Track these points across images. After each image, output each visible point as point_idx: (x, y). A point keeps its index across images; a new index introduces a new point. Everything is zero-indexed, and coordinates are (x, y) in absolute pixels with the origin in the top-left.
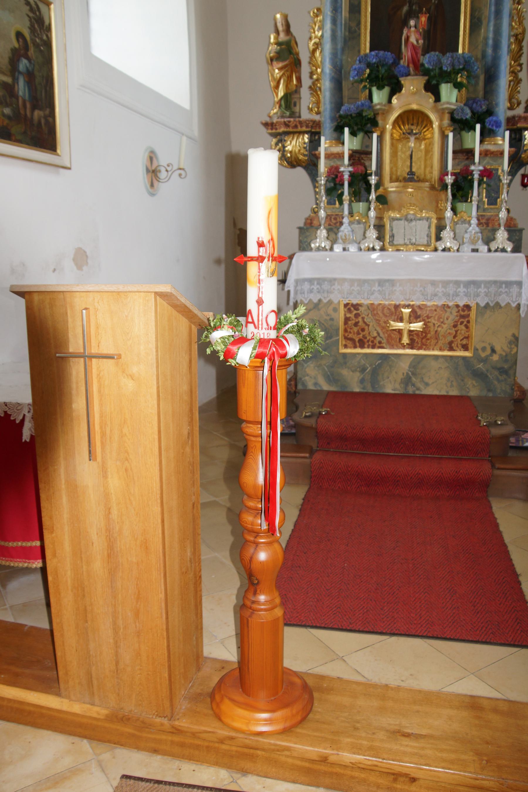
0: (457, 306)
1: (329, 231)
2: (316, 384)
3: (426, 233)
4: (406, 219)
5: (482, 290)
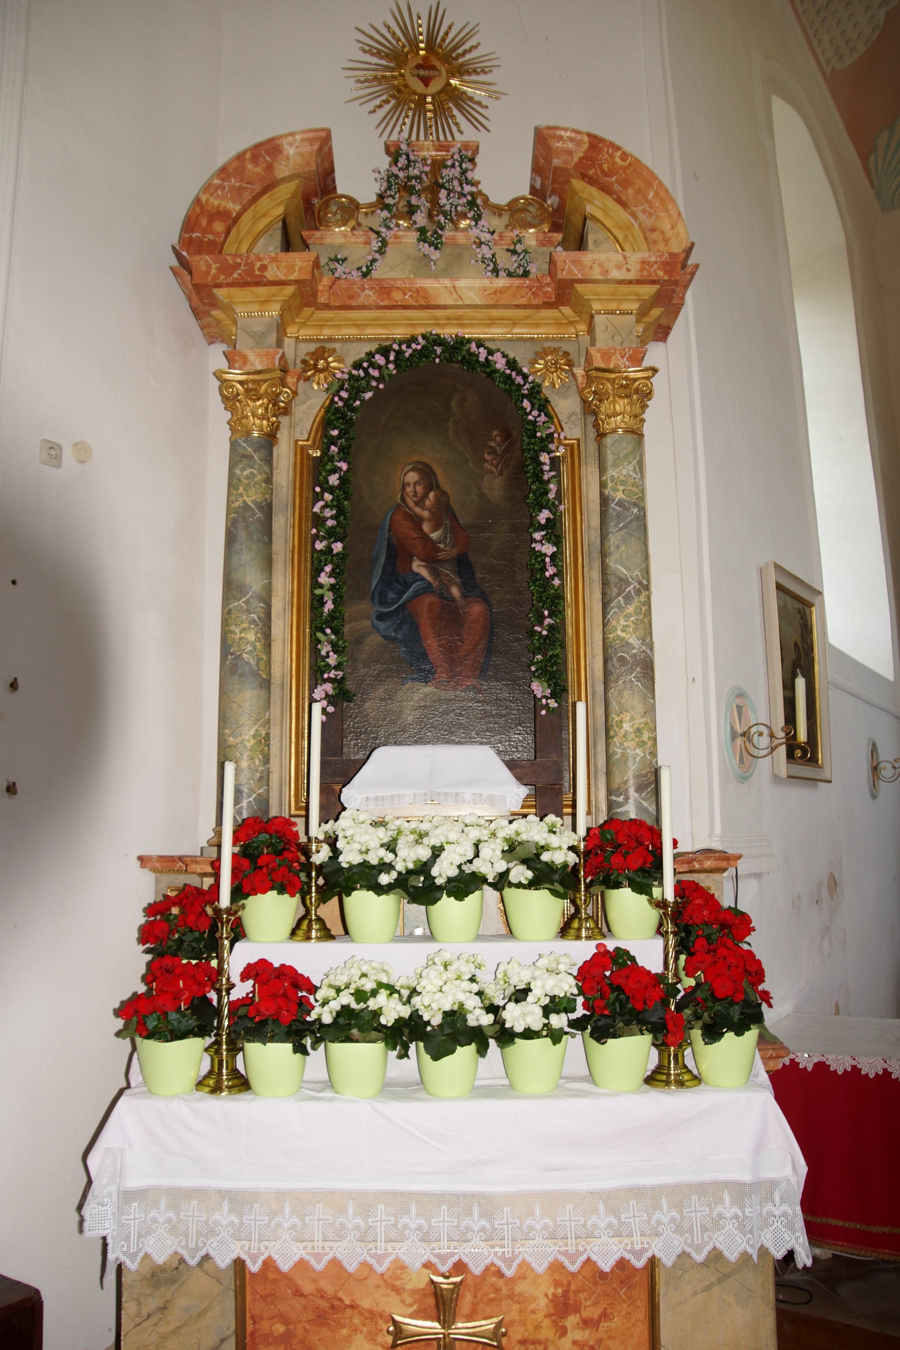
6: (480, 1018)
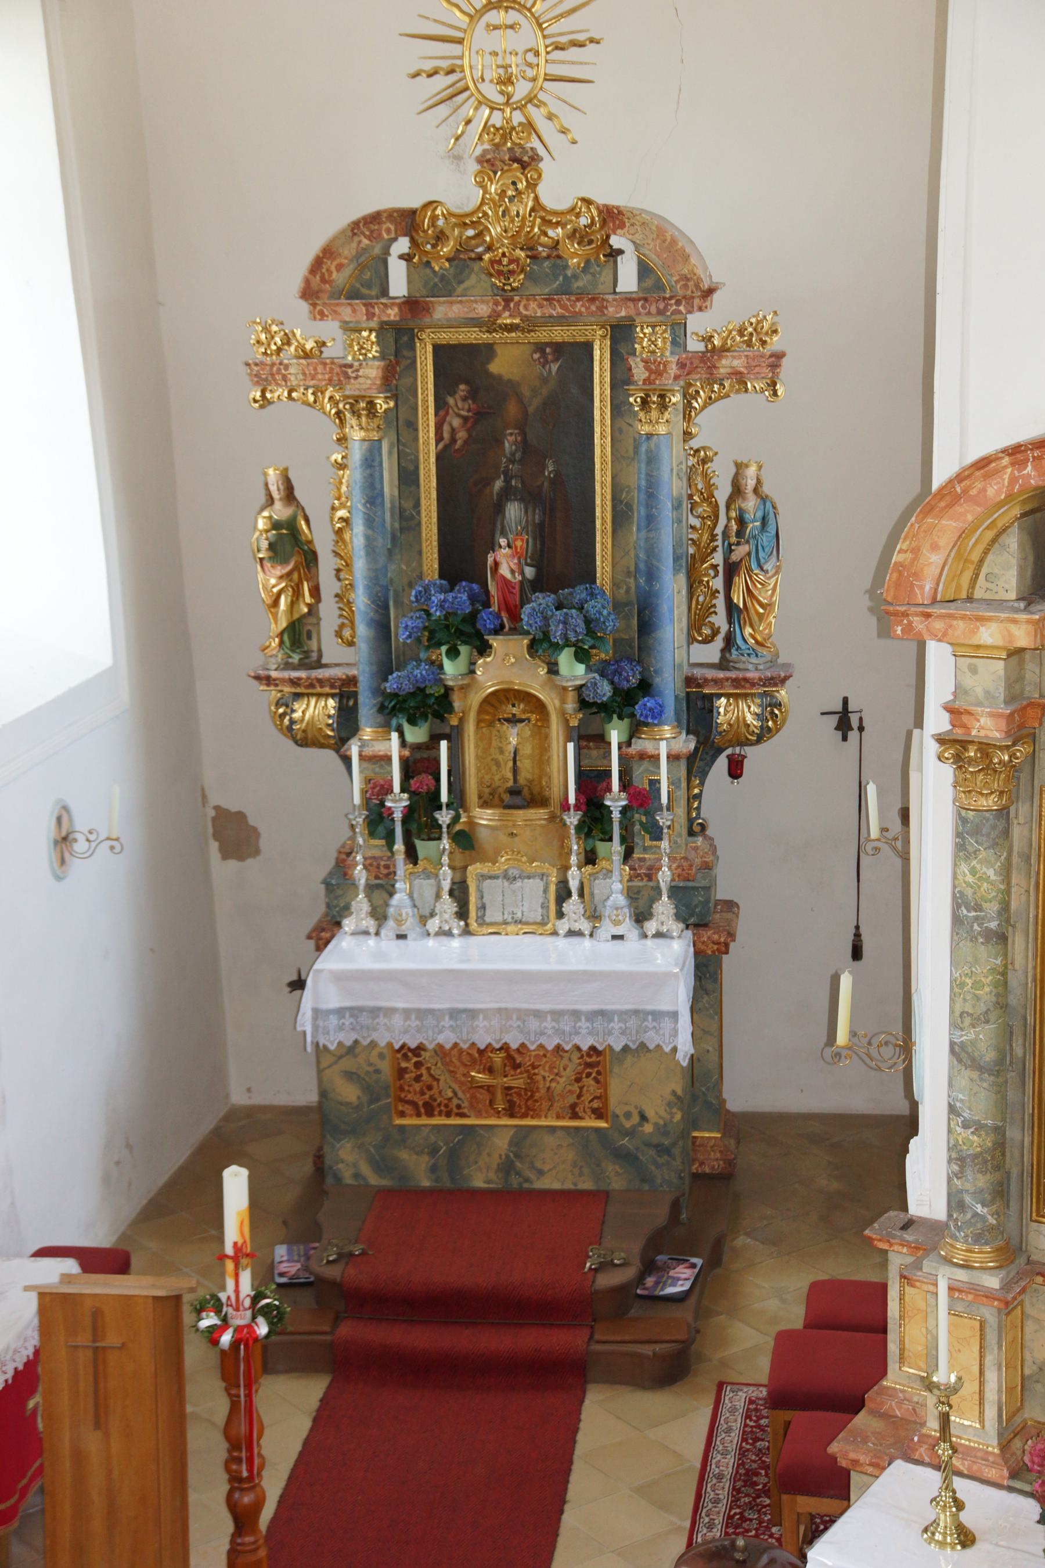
0: (578, 1048)
2: (357, 1176)
3: (541, 901)
4: (506, 876)
5: (616, 1025)
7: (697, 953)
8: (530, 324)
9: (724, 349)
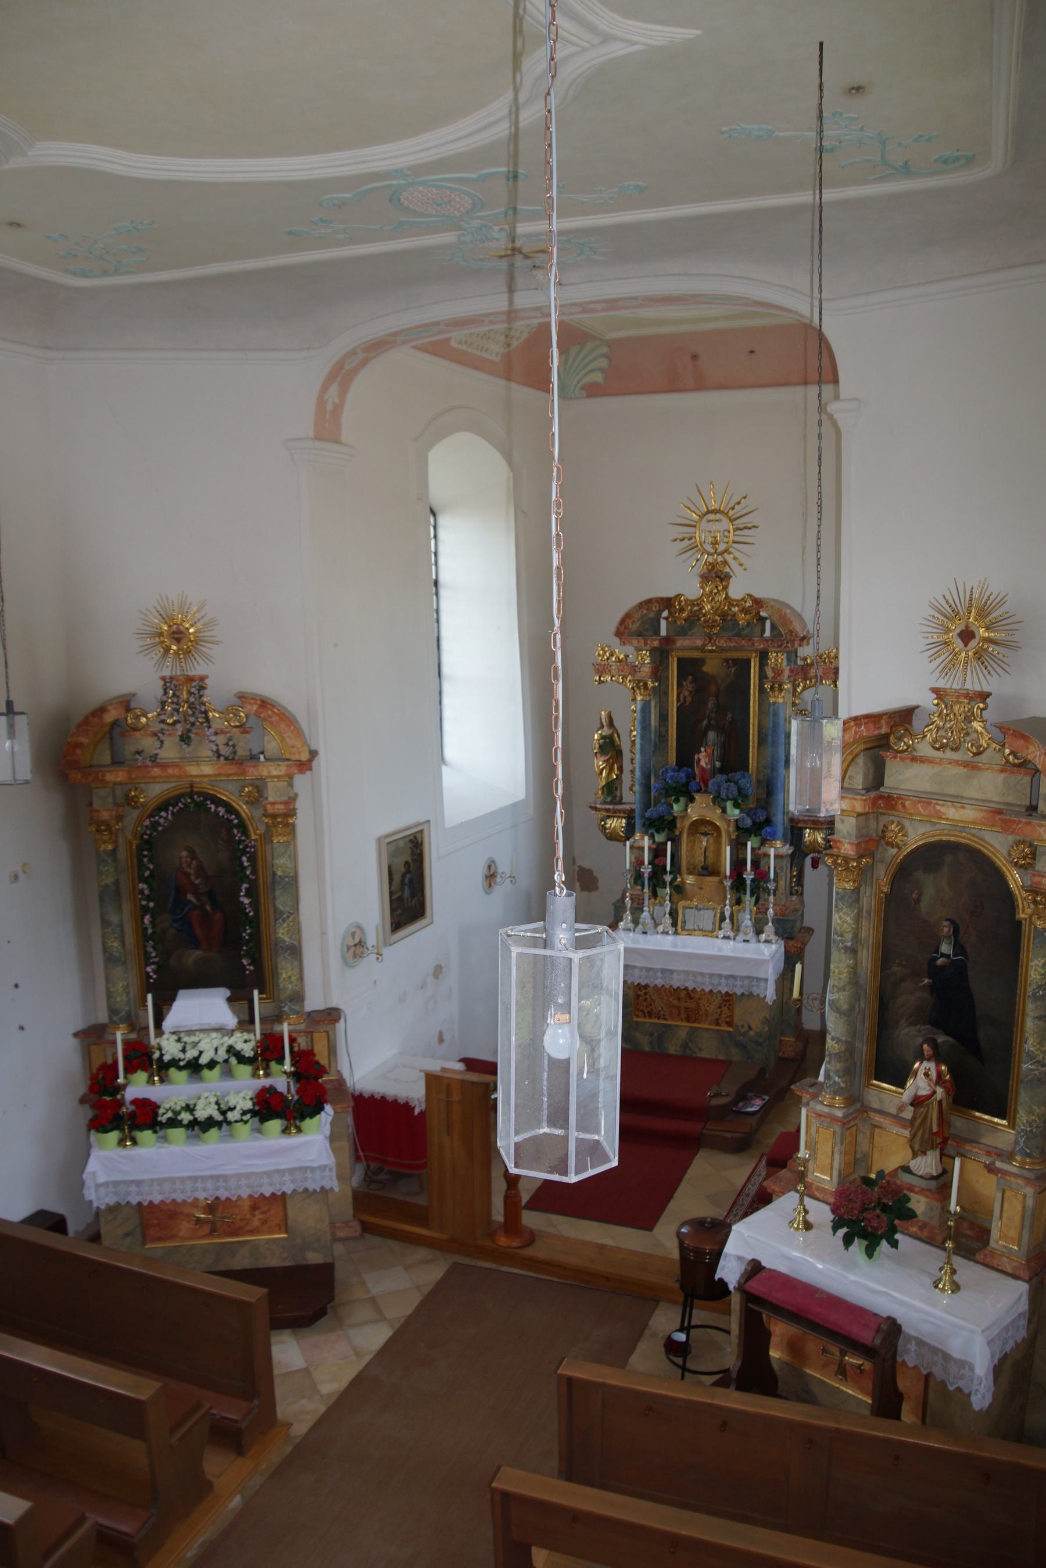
0: (720, 992)
1: (632, 914)
4: (697, 908)
5: (739, 983)
6: (219, 1117)
7: (786, 952)
8: (722, 650)
9: (812, 664)
